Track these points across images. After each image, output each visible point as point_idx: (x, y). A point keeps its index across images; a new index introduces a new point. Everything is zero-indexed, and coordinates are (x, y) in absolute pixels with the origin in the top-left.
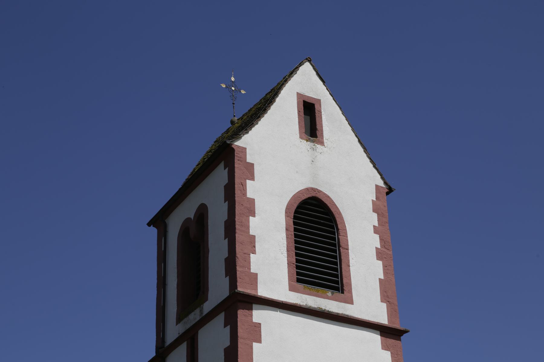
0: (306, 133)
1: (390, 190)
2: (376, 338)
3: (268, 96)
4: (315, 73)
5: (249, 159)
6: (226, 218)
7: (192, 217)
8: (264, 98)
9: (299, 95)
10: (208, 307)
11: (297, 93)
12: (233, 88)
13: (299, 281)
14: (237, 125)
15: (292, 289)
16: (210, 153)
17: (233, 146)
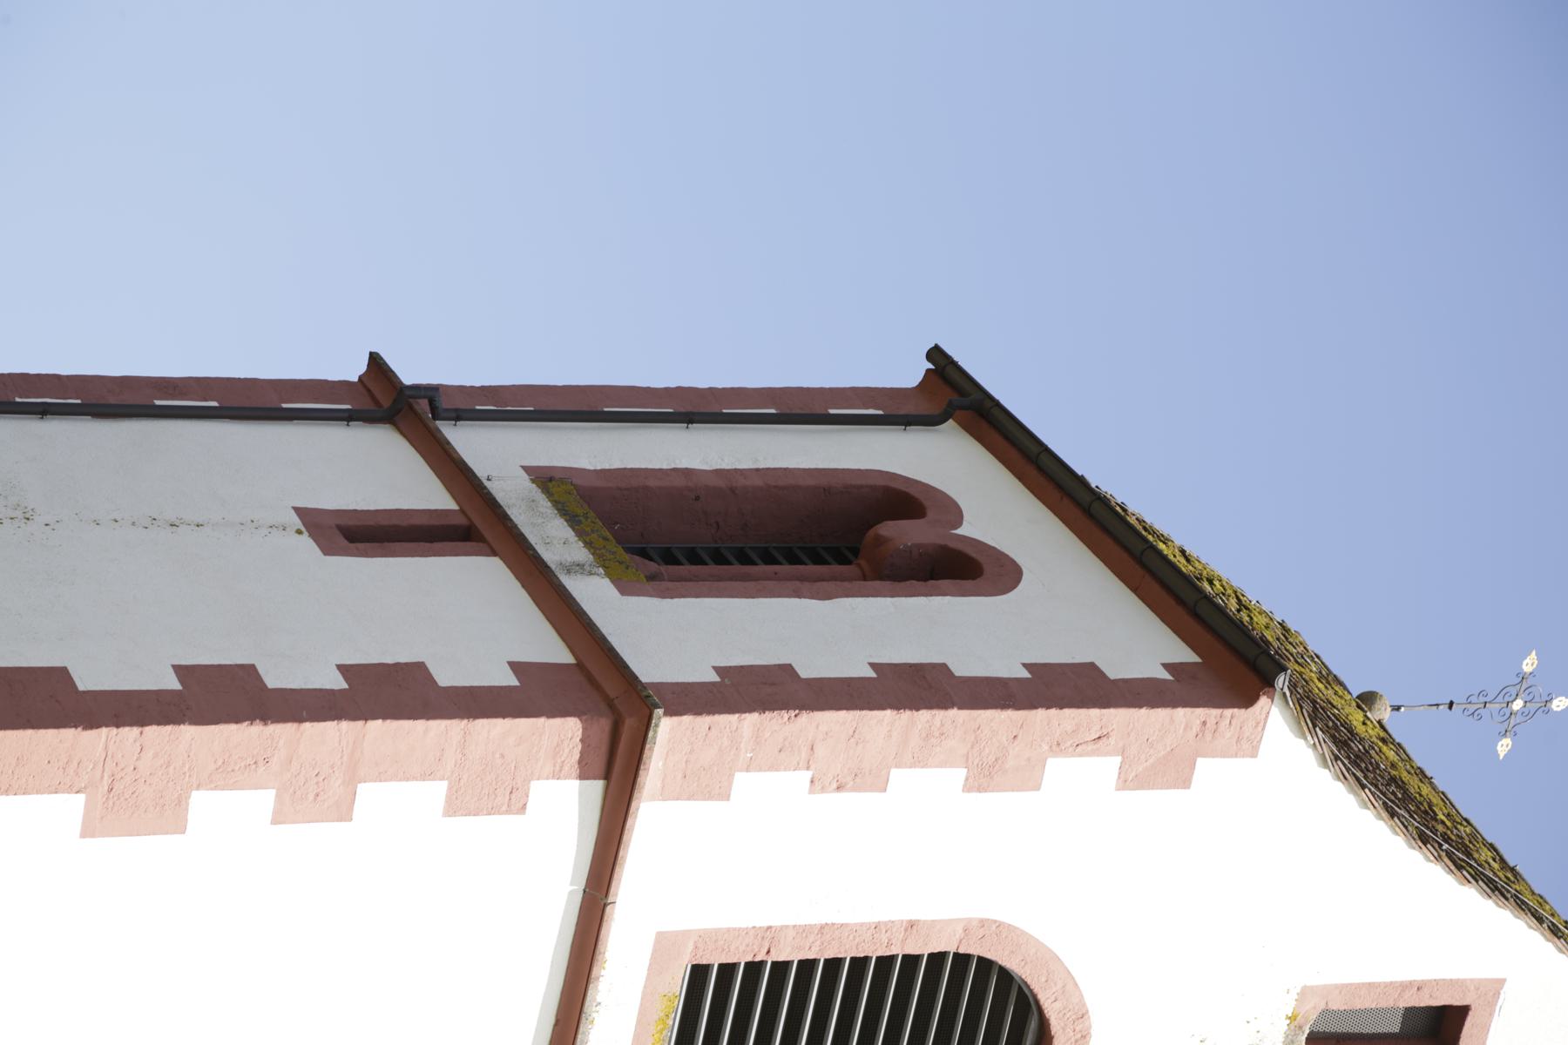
0: (1326, 1013)
3: (1485, 855)
6: (961, 669)
7: (963, 531)
8: (1475, 835)
9: (1494, 988)
11: (1502, 982)
12: (1518, 705)
13: (699, 973)
14: (1356, 718)
15: (665, 944)
16: (1233, 605)
17: (1263, 701)
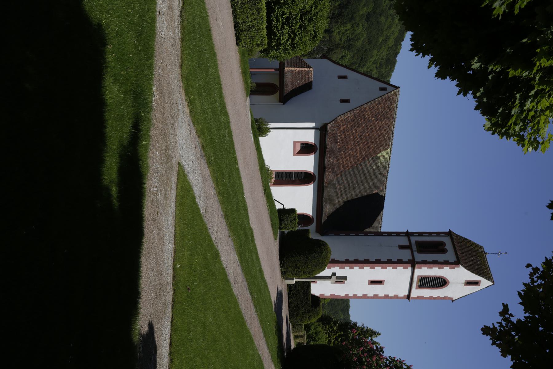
1: (453, 301)
2: (407, 293)
4: (483, 288)
5: (456, 268)
6: (439, 261)
7: (446, 247)
9: (480, 281)
10: (416, 253)
13: (421, 278)
15: (418, 276)
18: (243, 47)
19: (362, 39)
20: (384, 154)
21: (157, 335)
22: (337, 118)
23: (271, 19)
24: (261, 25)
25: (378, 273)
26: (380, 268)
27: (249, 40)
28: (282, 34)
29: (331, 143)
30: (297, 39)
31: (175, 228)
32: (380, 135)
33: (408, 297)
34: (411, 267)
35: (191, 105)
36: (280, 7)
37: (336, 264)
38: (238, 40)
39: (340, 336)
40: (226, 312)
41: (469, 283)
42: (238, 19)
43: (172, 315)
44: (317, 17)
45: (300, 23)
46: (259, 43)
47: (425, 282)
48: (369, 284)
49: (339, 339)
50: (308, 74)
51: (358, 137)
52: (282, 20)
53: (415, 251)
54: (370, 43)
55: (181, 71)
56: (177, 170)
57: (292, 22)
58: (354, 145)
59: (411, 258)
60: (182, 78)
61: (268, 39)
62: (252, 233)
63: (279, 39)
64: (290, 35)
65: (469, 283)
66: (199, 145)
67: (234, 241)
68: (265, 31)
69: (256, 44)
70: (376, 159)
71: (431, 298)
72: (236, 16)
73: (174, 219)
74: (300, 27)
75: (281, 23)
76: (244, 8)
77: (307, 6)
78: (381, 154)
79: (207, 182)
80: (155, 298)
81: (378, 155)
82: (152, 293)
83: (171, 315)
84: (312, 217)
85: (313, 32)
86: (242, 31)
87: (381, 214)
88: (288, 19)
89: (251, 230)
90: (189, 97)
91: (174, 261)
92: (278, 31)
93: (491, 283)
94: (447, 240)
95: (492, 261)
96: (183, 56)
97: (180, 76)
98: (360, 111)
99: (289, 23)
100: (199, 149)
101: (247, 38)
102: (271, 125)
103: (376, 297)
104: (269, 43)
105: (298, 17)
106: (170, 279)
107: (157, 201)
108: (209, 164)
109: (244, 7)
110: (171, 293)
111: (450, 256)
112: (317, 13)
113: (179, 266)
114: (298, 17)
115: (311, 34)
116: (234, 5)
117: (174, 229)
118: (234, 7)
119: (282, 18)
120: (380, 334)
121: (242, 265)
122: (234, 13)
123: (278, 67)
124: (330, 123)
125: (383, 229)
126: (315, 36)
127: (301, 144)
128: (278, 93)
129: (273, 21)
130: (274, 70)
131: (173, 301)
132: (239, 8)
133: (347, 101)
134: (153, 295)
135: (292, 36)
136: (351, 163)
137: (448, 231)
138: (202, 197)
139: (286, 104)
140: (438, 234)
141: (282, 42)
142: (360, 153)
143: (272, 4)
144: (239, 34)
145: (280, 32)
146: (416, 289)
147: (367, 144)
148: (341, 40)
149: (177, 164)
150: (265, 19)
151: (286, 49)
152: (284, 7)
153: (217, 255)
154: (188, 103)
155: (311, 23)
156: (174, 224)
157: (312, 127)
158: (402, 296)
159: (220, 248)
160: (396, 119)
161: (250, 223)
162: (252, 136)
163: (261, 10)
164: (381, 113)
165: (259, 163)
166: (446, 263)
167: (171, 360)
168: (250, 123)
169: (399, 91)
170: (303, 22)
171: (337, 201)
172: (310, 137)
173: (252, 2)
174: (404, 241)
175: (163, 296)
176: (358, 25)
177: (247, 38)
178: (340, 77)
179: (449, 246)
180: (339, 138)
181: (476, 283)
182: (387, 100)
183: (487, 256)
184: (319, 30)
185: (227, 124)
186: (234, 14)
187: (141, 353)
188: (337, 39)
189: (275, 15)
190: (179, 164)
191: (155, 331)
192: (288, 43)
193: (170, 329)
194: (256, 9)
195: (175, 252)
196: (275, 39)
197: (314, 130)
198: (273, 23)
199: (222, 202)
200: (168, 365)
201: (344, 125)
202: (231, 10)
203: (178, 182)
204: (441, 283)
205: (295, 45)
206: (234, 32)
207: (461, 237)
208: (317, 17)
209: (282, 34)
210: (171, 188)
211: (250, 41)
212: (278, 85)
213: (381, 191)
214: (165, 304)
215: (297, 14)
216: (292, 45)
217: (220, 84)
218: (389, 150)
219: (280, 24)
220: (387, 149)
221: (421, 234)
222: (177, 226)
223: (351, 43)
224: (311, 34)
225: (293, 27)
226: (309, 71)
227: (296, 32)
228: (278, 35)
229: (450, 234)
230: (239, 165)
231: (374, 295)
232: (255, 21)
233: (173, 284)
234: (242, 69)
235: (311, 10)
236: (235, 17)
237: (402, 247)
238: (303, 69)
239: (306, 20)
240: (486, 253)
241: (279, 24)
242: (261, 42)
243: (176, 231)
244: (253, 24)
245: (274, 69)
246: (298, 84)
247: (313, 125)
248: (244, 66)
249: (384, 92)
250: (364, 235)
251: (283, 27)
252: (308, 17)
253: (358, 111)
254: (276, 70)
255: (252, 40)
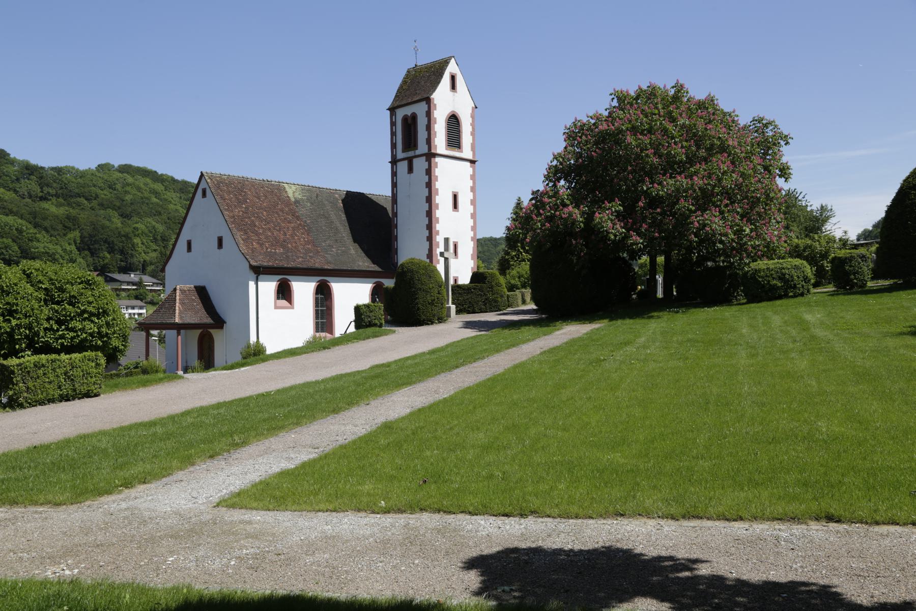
2: (468, 164)
9: (450, 73)
15: (446, 149)
18: (100, 388)
19: (154, 223)
20: (291, 192)
21: (487, 547)
22: (243, 254)
23: (59, 347)
24: (64, 361)
25: (443, 200)
26: (437, 197)
27: (89, 379)
28: (83, 330)
29: (275, 260)
30: (90, 309)
31: (320, 511)
32: (266, 196)
33: (473, 162)
34: (435, 157)
35: (131, 483)
36: (37, 334)
37: (434, 252)
38: (88, 395)
39: (523, 248)
40: (475, 408)
41: (453, 87)
42: (53, 396)
43: (462, 512)
44: (56, 280)
45: (66, 305)
46: (93, 364)
47: (454, 140)
48: (458, 211)
49: (527, 248)
50: (185, 291)
51: (268, 226)
52: (61, 331)
53: (415, 153)
54: (160, 214)
55: (64, 504)
56: (225, 509)
57: (63, 316)
58: (279, 231)
59: (424, 158)
60: (77, 503)
61: (87, 351)
62: (377, 366)
63: (91, 335)
64: (84, 319)
65: (453, 87)
66: (209, 463)
67: (377, 396)
68: (74, 356)
69: (96, 368)
70: (297, 202)
71: (473, 134)
72: (50, 399)
73: (304, 513)
74: (70, 304)
75: (66, 333)
76: (36, 388)
77: (36, 294)
78: (291, 195)
79: (273, 446)
80: (424, 556)
81: (293, 199)
82: (413, 564)
83: (461, 516)
84: (278, 281)
85: (81, 286)
86: (75, 390)
87: (370, 196)
88: (60, 322)
89: (372, 368)
90: (117, 486)
91: (373, 512)
92: (78, 336)
93: (453, 61)
94: (401, 113)
95: (426, 58)
96: (41, 502)
97: (72, 507)
98: (233, 223)
99: (67, 321)
100: (219, 462)
101: (86, 381)
102: (253, 339)
103: (473, 202)
104: (96, 348)
105: (56, 307)
106: (401, 519)
107: (255, 557)
108: (244, 443)
109: (33, 388)
110: (425, 516)
111: (419, 109)
112: (51, 279)
113: (383, 502)
114: (56, 308)
115: (83, 288)
116: (30, 404)
117: (320, 514)
118: (34, 404)
119: (58, 330)
120: (519, 198)
121: (415, 383)
122: (44, 403)
123: (175, 331)
124: (249, 262)
125: (389, 194)
126: (87, 282)
127: (278, 298)
128: (212, 331)
129: (62, 344)
130: (180, 337)
131: (439, 511)
132: (34, 395)
133: (220, 241)
134: (417, 562)
135: (86, 315)
136: (303, 233)
137: (389, 112)
138: (292, 456)
139: (225, 320)
140: (393, 124)
141: (96, 330)
142: (289, 222)
143: (37, 345)
144: (79, 394)
145: (80, 333)
146: (462, 152)
147: (277, 213)
148: (155, 250)
149: (216, 510)
150: (54, 356)
151: (108, 324)
152: (36, 329)
153: (387, 427)
154: (126, 488)
155: (66, 289)
156: (312, 514)
157: (255, 286)
158: (471, 169)
159: (381, 420)
160: (245, 176)
161: (364, 368)
162: (243, 369)
163: (38, 363)
164: (236, 195)
165: (285, 357)
166: (429, 114)
167: (533, 512)
168: (225, 372)
169: (207, 173)
170: (65, 300)
171: (353, 252)
172: (268, 287)
173: (24, 376)
174: (403, 167)
175: (425, 536)
176: (136, 229)
177: (86, 381)
178: (189, 249)
179: (408, 111)
180: (269, 250)
181: (453, 78)
182: (219, 188)
183: (419, 64)
184: (78, 277)
185: (203, 411)
186: (46, 402)
187: (514, 588)
188: (154, 255)
189: (54, 342)
190: (218, 505)
191: (480, 553)
192: (97, 321)
193: (482, 517)
194: (36, 371)
195: (359, 510)
196: (92, 341)
197: (259, 283)
198: (65, 344)
199: (313, 418)
200: (541, 520)
201: (253, 245)
202: (39, 408)
203: (246, 508)
204: (454, 121)
205: (101, 310)
206: (77, 401)
207: (396, 96)
208: (56, 280)
209: (83, 330)
210: (250, 523)
211: (91, 377)
212: (200, 331)
213: (340, 195)
214: (439, 531)
215: (52, 309)
216: (98, 316)
217: (130, 427)
218: (286, 185)
219: (68, 334)
220: (285, 188)
221: (394, 146)
222: (317, 508)
223: (159, 238)
224: (83, 288)
225: (72, 315)
226: (180, 290)
227: (79, 311)
228: (85, 335)
229: (392, 110)
230: (271, 390)
231: (472, 204)
232: (58, 370)
233: (411, 513)
234: (138, 387)
235: (46, 289)
236: (51, 401)
237: (410, 170)
238: (178, 298)
239: (61, 296)
240: (416, 65)
241: (67, 336)
242: (92, 361)
243: (325, 510)
244: (61, 374)
245: (178, 336)
246: (198, 304)
247: (252, 285)
248: (134, 383)
249: (208, 191)
250: (397, 217)
251: (72, 330)
252: (57, 292)
253: (233, 226)
254: (179, 334)
255: (89, 374)
